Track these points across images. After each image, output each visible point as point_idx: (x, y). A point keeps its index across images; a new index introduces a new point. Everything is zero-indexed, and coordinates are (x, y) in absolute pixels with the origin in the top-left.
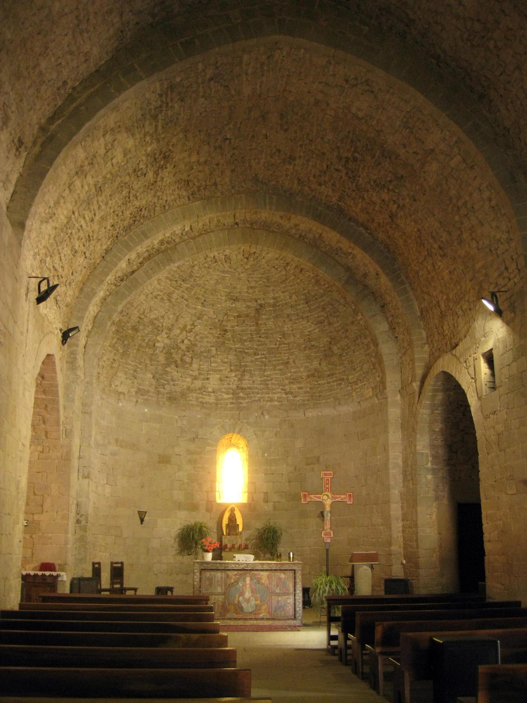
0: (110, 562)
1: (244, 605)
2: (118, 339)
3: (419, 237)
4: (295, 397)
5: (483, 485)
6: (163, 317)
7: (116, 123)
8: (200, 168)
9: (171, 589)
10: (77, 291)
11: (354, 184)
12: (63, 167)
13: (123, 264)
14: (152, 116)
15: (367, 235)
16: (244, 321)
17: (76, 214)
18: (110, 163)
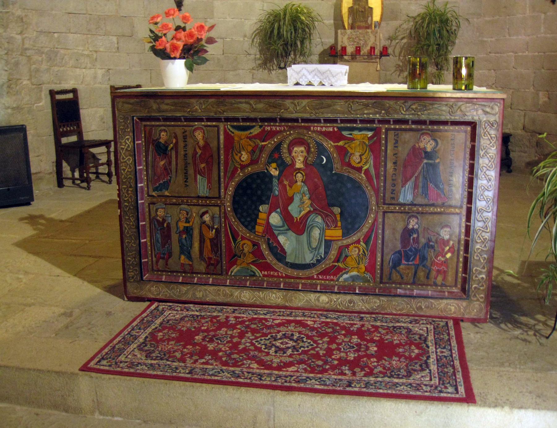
0: (109, 87)
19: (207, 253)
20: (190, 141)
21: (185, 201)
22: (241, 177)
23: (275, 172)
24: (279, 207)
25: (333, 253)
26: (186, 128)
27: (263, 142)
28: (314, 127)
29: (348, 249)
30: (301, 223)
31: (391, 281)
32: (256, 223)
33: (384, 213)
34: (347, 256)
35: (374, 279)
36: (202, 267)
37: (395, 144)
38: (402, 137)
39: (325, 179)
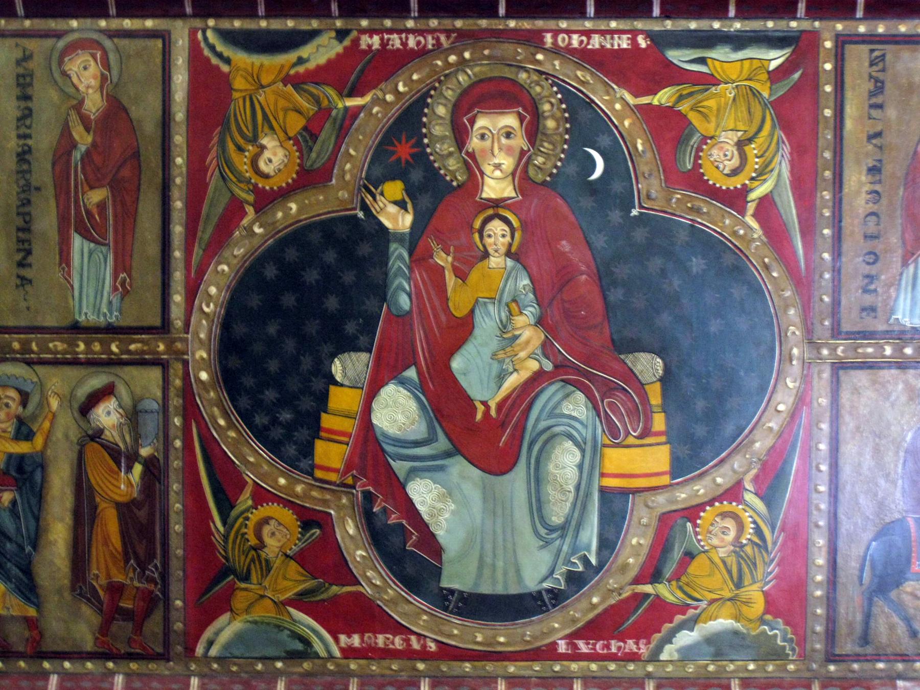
1: (442, 500)
19: (104, 568)
20: (46, 98)
21: (16, 345)
22: (256, 242)
24: (416, 363)
25: (637, 542)
26: (32, 45)
27: (352, 94)
28: (556, 33)
29: (695, 525)
30: (503, 425)
31: (869, 650)
32: (316, 430)
33: (839, 367)
34: (689, 556)
35: (802, 641)
36: (83, 629)
37: (872, 94)
38: (900, 67)
39: (600, 241)
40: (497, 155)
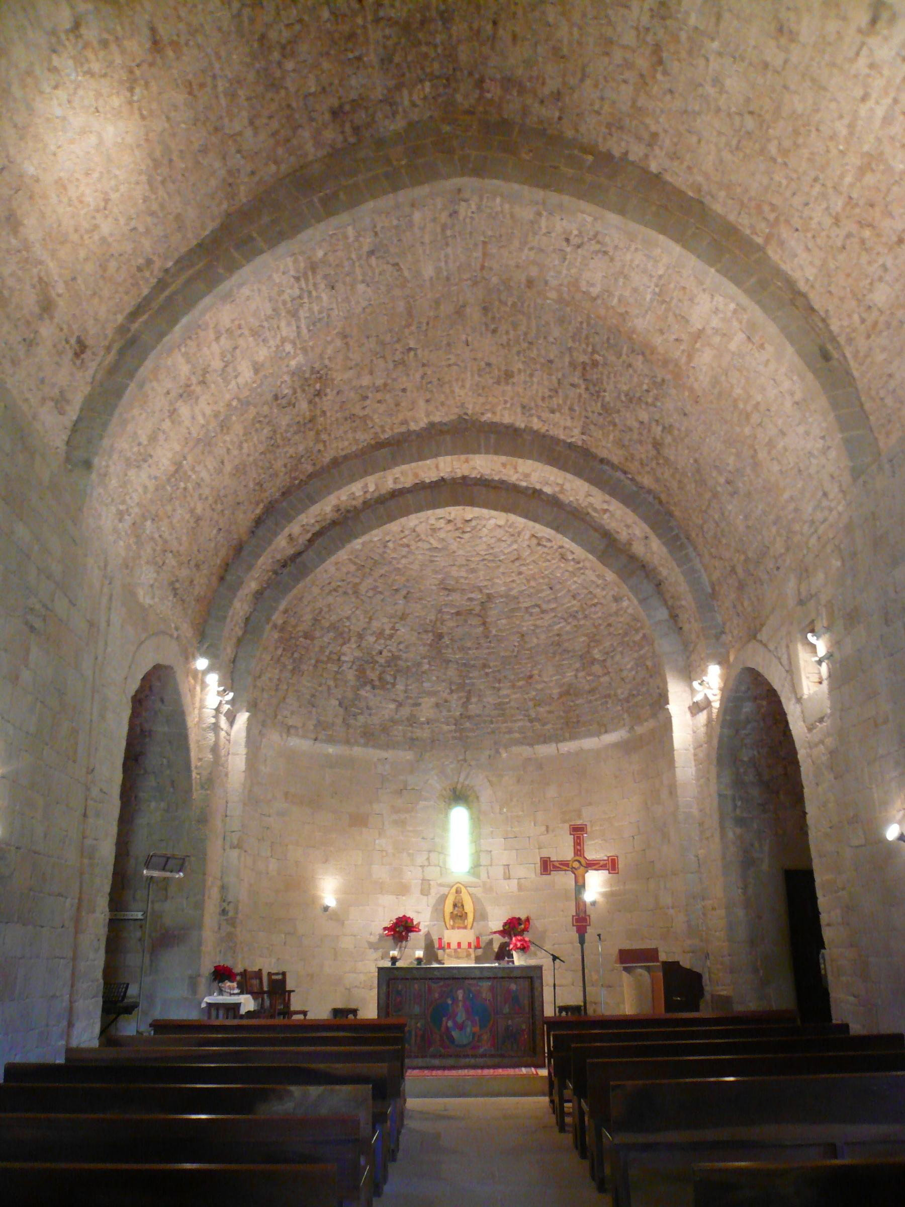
2: (284, 650)
3: (698, 471)
4: (544, 725)
5: (813, 834)
6: (348, 618)
7: (233, 321)
8: (379, 396)
9: (354, 1012)
10: (214, 579)
11: (599, 404)
12: (155, 384)
13: (281, 541)
14: (289, 312)
15: (629, 482)
16: (466, 621)
17: (189, 458)
18: (233, 383)
23: (450, 1002)
40: (460, 994)
